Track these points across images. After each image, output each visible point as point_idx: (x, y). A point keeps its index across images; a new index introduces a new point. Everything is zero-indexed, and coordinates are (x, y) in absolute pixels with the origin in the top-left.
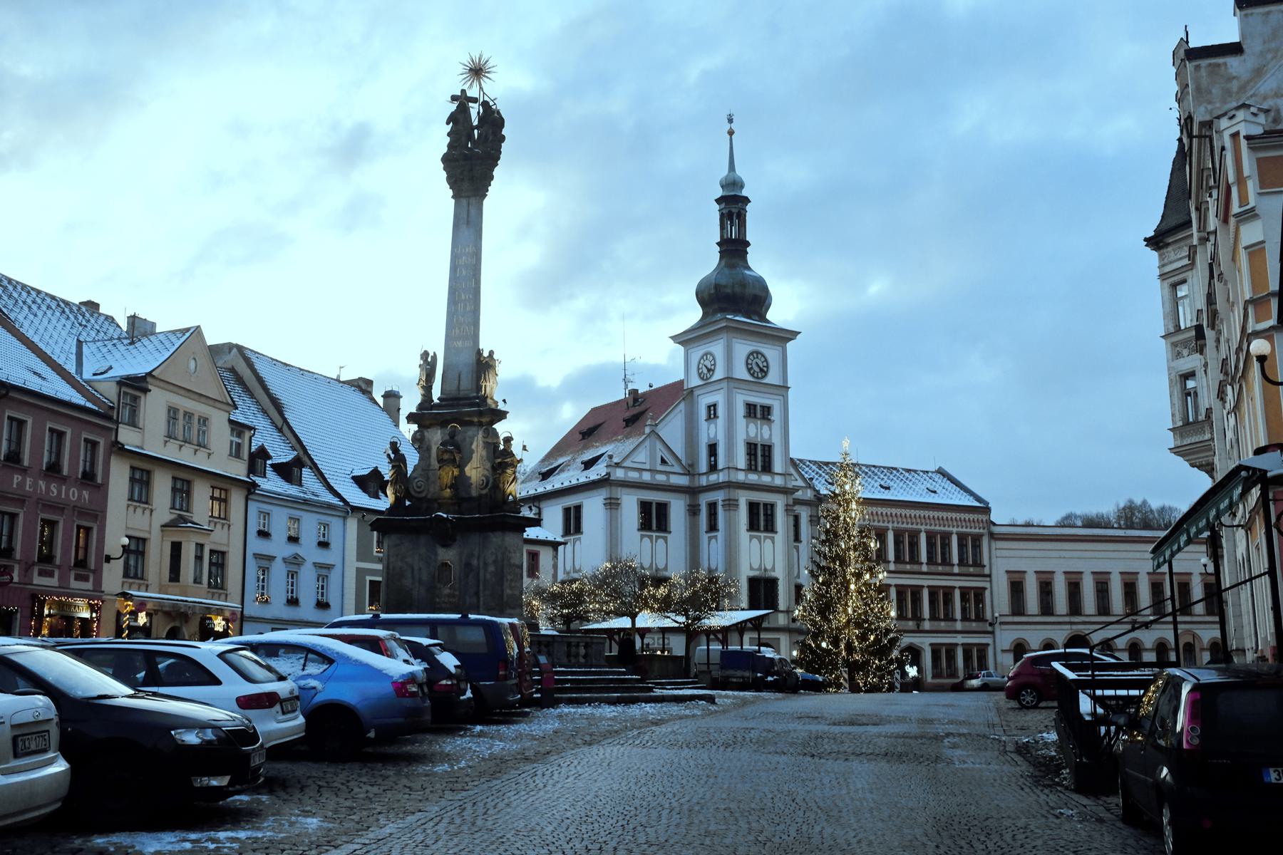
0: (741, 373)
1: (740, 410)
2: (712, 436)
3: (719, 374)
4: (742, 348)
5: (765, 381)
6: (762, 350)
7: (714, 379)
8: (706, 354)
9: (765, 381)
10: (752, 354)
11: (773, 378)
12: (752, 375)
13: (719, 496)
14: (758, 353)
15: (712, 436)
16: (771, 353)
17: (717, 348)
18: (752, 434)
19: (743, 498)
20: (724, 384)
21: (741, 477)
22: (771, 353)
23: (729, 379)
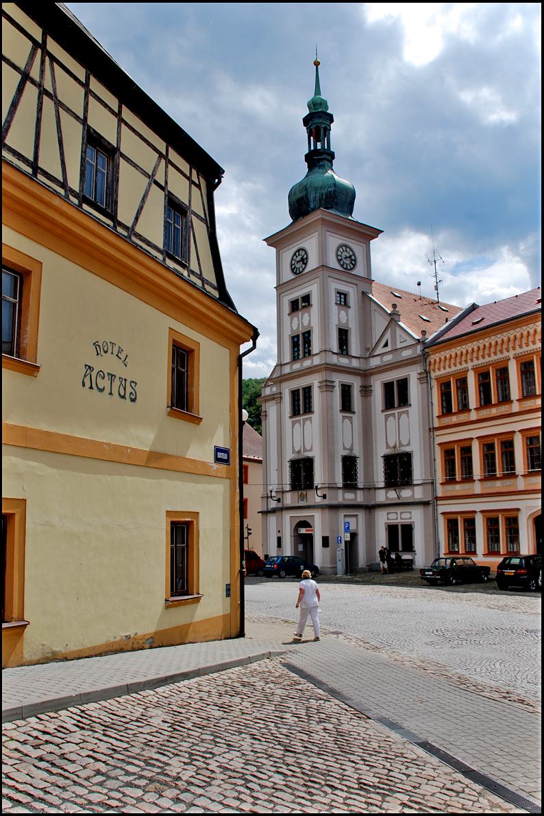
0: (334, 263)
1: (333, 298)
2: (306, 323)
3: (313, 263)
4: (334, 241)
5: (354, 272)
6: (352, 246)
7: (306, 271)
8: (298, 251)
9: (354, 272)
10: (341, 246)
11: (359, 270)
12: (342, 266)
13: (315, 381)
14: (346, 246)
15: (306, 323)
16: (358, 249)
17: (311, 244)
18: (344, 321)
19: (338, 379)
20: (320, 273)
21: (335, 360)
22: (358, 249)
23: (323, 267)
